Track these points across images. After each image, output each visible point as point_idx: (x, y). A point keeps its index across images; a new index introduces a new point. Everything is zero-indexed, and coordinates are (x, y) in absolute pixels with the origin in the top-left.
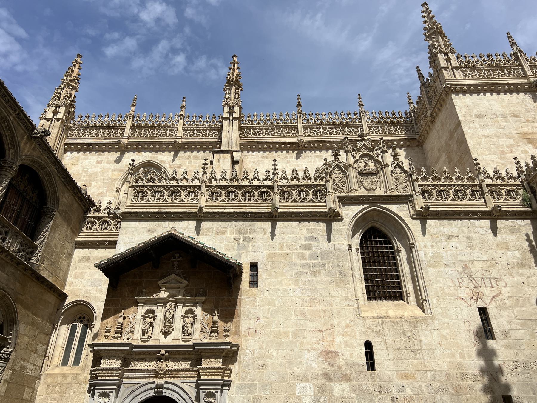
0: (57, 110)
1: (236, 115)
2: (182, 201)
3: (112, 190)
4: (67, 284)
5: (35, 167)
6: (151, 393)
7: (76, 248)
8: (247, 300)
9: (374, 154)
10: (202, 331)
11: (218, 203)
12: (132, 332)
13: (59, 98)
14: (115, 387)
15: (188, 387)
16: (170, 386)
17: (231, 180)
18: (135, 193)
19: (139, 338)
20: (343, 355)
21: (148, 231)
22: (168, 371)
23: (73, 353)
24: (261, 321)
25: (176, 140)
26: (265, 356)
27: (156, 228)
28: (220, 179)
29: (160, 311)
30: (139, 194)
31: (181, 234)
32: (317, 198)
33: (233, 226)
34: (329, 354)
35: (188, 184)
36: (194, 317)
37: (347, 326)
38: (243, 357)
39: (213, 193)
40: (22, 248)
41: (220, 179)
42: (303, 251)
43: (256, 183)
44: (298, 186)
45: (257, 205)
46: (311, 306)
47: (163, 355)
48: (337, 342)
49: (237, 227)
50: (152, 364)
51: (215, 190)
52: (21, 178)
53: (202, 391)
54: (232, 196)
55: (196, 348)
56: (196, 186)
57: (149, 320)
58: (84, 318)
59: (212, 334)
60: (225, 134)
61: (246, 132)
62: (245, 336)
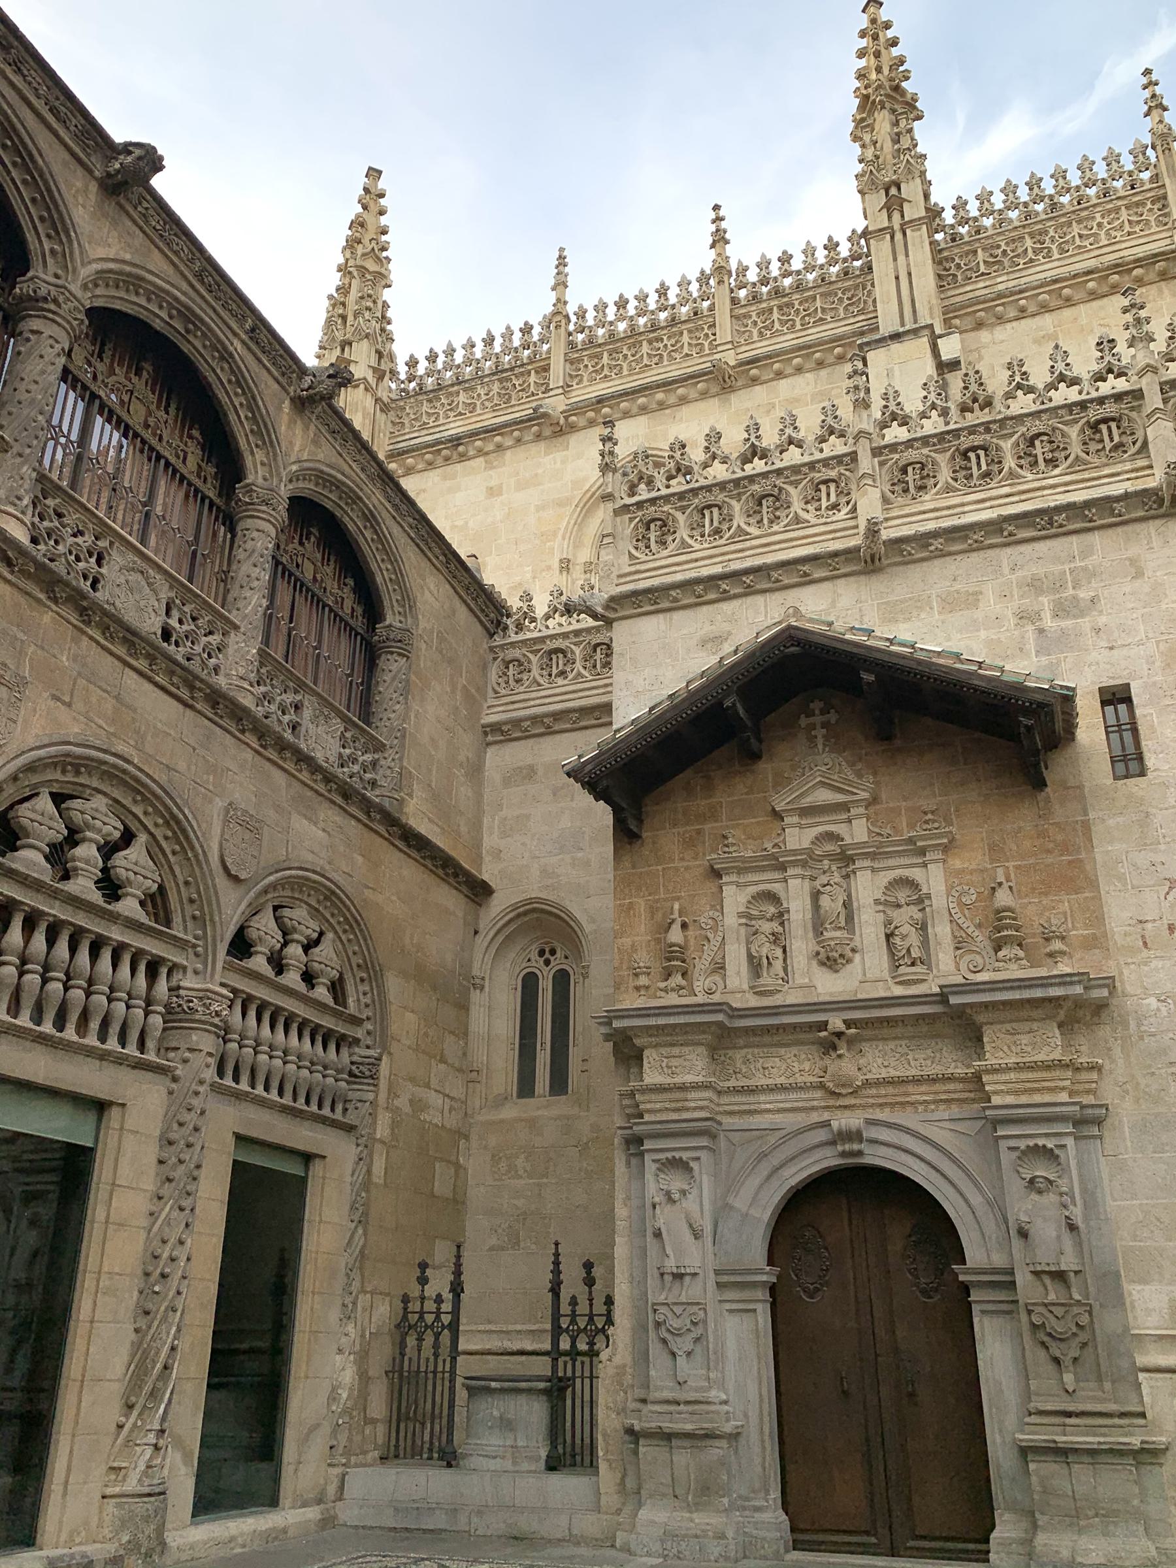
0: (346, 355)
1: (915, 211)
2: (797, 520)
3: (549, 568)
4: (487, 858)
5: (329, 500)
6: (827, 1159)
7: (488, 744)
8: (1111, 822)
10: (959, 945)
11: (928, 500)
12: (719, 968)
13: (344, 318)
14: (704, 1142)
15: (949, 1134)
16: (884, 1135)
17: (964, 409)
18: (636, 528)
19: (745, 987)
21: (703, 643)
22: (867, 1084)
23: (543, 1057)
27: (726, 627)
28: (924, 415)
29: (796, 895)
30: (648, 529)
31: (823, 623)
33: (1006, 571)
35: (807, 459)
36: (920, 901)
38: (1139, 1025)
39: (904, 471)
40: (348, 751)
41: (924, 415)
43: (1065, 395)
45: (1086, 475)
47: (839, 1035)
49: (1020, 573)
50: (807, 1066)
51: (912, 455)
52: (301, 543)
53: (1003, 1145)
55: (953, 1000)
56: (839, 459)
57: (767, 927)
58: (553, 952)
59: (1001, 954)
61: (958, 266)
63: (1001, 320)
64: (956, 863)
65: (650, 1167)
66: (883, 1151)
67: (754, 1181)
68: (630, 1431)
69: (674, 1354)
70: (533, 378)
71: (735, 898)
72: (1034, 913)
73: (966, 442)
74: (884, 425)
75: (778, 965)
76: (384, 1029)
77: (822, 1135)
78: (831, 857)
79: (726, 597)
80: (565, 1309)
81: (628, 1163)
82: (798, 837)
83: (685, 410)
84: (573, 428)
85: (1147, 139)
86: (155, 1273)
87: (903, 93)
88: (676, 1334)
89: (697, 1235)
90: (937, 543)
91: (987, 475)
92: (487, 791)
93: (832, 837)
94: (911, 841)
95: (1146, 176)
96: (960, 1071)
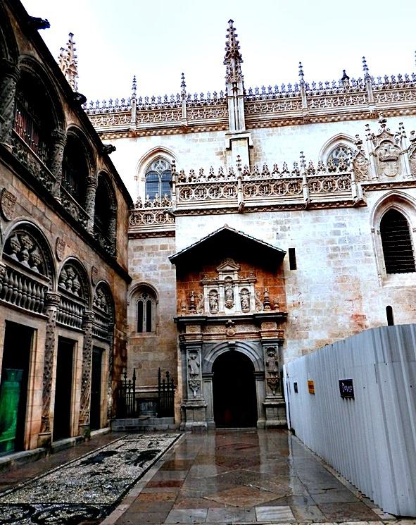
6: (227, 350)
7: (129, 239)
9: (393, 139)
10: (257, 304)
16: (239, 345)
20: (369, 317)
22: (236, 334)
23: (145, 323)
24: (302, 295)
25: (183, 123)
26: (308, 321)
27: (203, 222)
32: (342, 187)
34: (358, 318)
37: (372, 296)
39: (248, 188)
42: (334, 237)
43: (286, 176)
44: (325, 177)
46: (342, 282)
47: (230, 324)
48: (364, 308)
51: (251, 185)
54: (266, 189)
56: (234, 183)
60: (232, 115)
62: (291, 307)
63: (259, 127)
64: (256, 286)
65: (187, 352)
66: (238, 348)
67: (211, 354)
68: (183, 407)
69: (193, 392)
70: (125, 117)
71: (206, 291)
72: (275, 298)
73: (263, 184)
74: (244, 175)
75: (216, 307)
76: (115, 317)
77: (226, 345)
78: (229, 282)
79: (205, 214)
80: (162, 382)
81: (181, 351)
82: (222, 278)
83: (172, 136)
84: (139, 136)
85: (299, 83)
86: (84, 379)
87: (238, 53)
88: (195, 387)
89: (199, 366)
90: (256, 209)
91: (267, 193)
92: (129, 253)
93: (228, 277)
94: (248, 280)
95: (298, 93)
96: (255, 331)
